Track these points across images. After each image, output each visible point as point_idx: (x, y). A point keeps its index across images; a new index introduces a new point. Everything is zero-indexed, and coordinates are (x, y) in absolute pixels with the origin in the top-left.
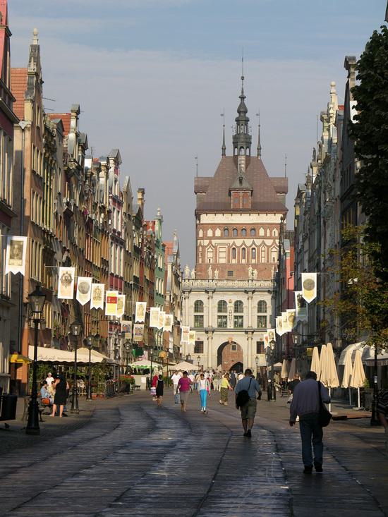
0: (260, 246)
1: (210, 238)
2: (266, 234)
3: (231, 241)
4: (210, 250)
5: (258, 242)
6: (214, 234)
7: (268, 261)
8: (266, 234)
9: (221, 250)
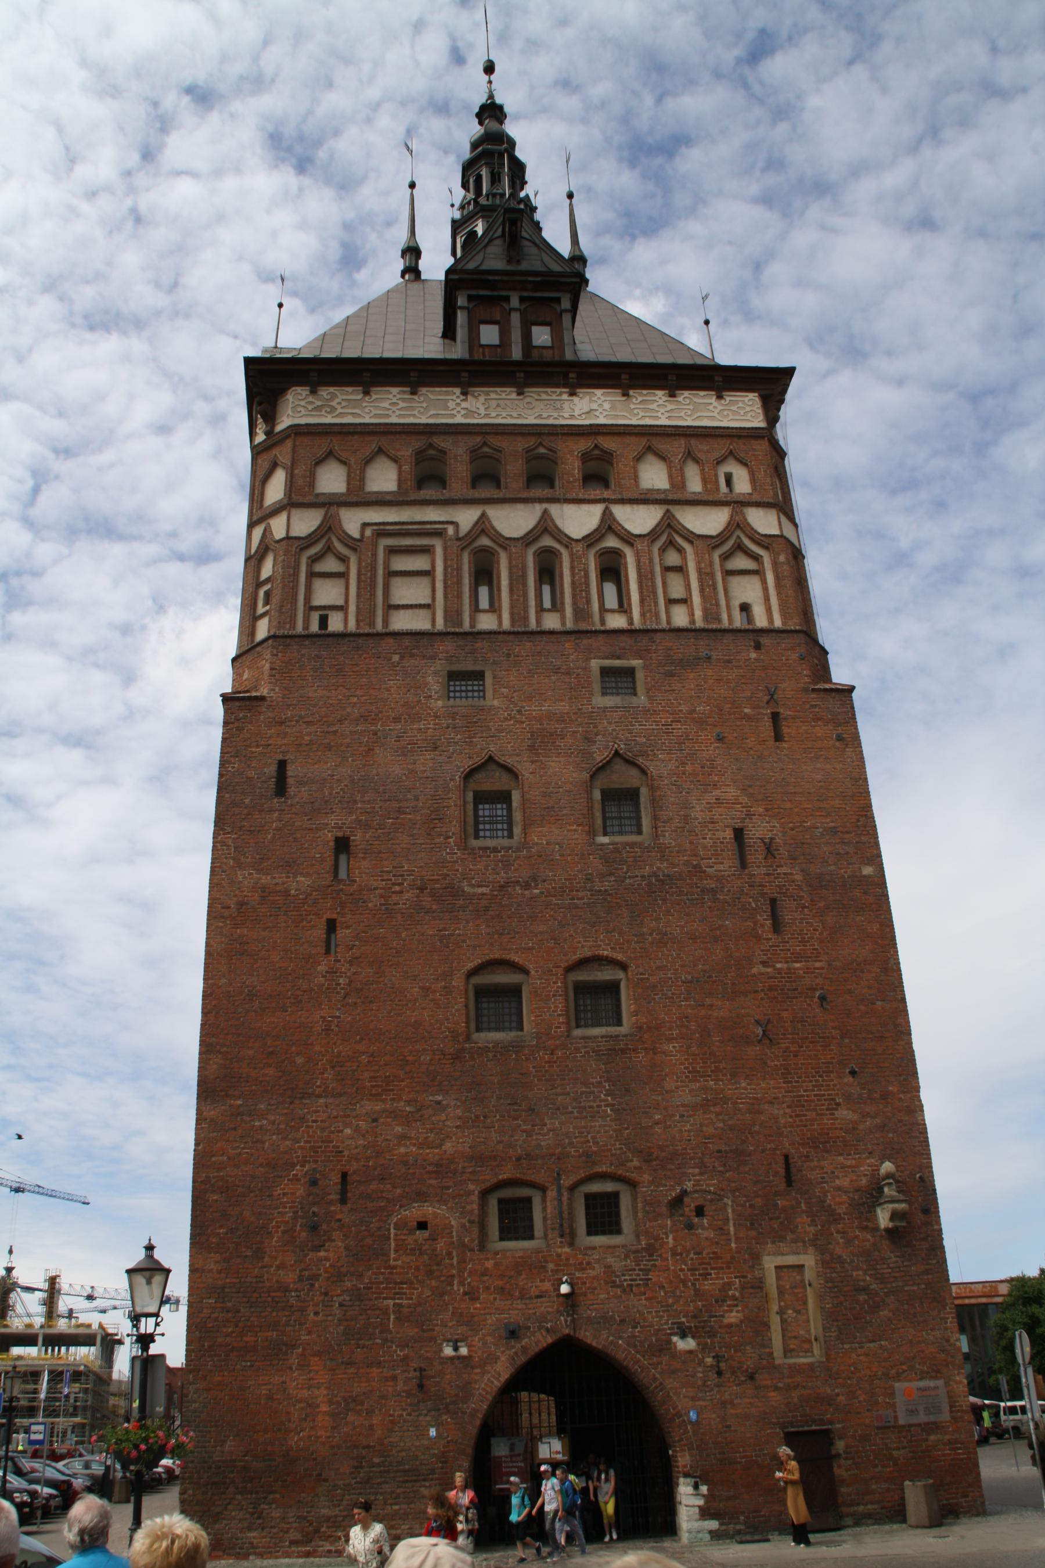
0: (653, 535)
1: (331, 503)
2: (678, 482)
3: (466, 518)
4: (330, 565)
5: (639, 520)
6: (356, 480)
7: (711, 612)
8: (678, 482)
9: (401, 563)
